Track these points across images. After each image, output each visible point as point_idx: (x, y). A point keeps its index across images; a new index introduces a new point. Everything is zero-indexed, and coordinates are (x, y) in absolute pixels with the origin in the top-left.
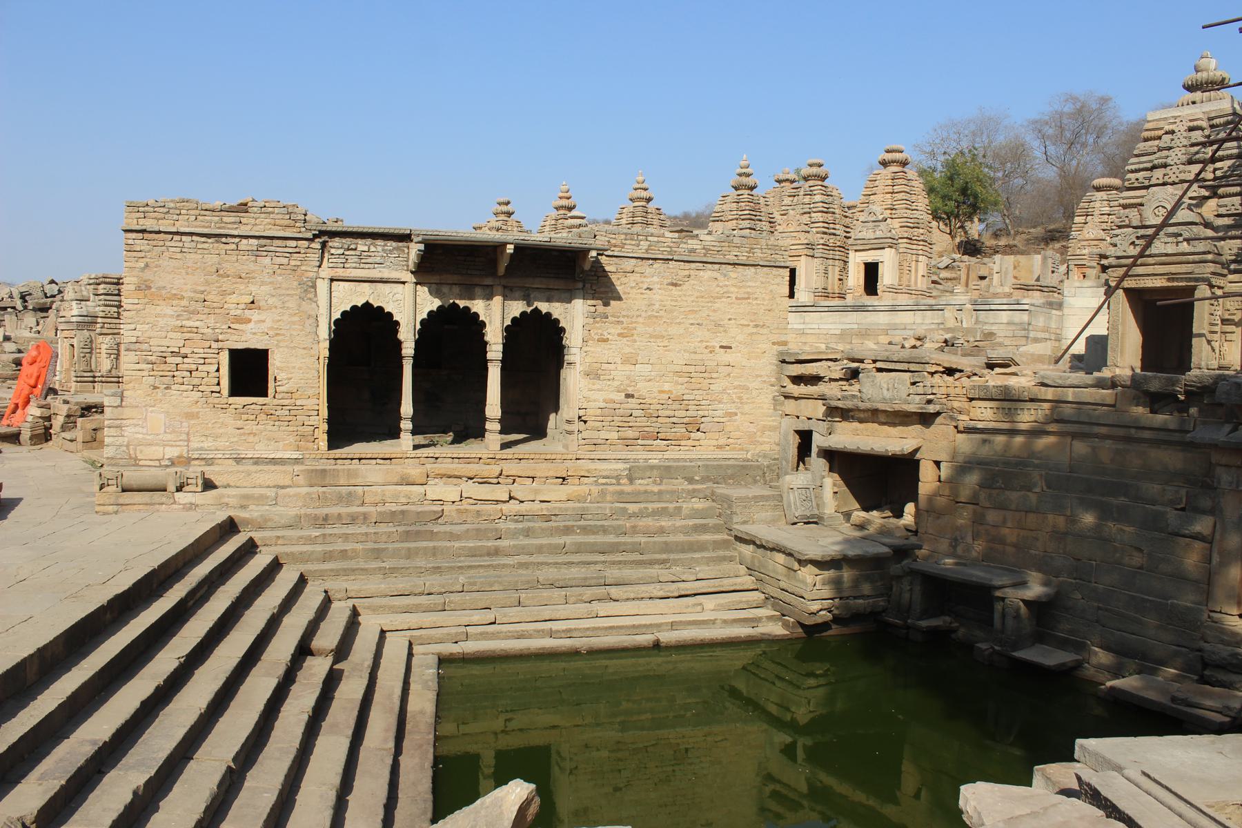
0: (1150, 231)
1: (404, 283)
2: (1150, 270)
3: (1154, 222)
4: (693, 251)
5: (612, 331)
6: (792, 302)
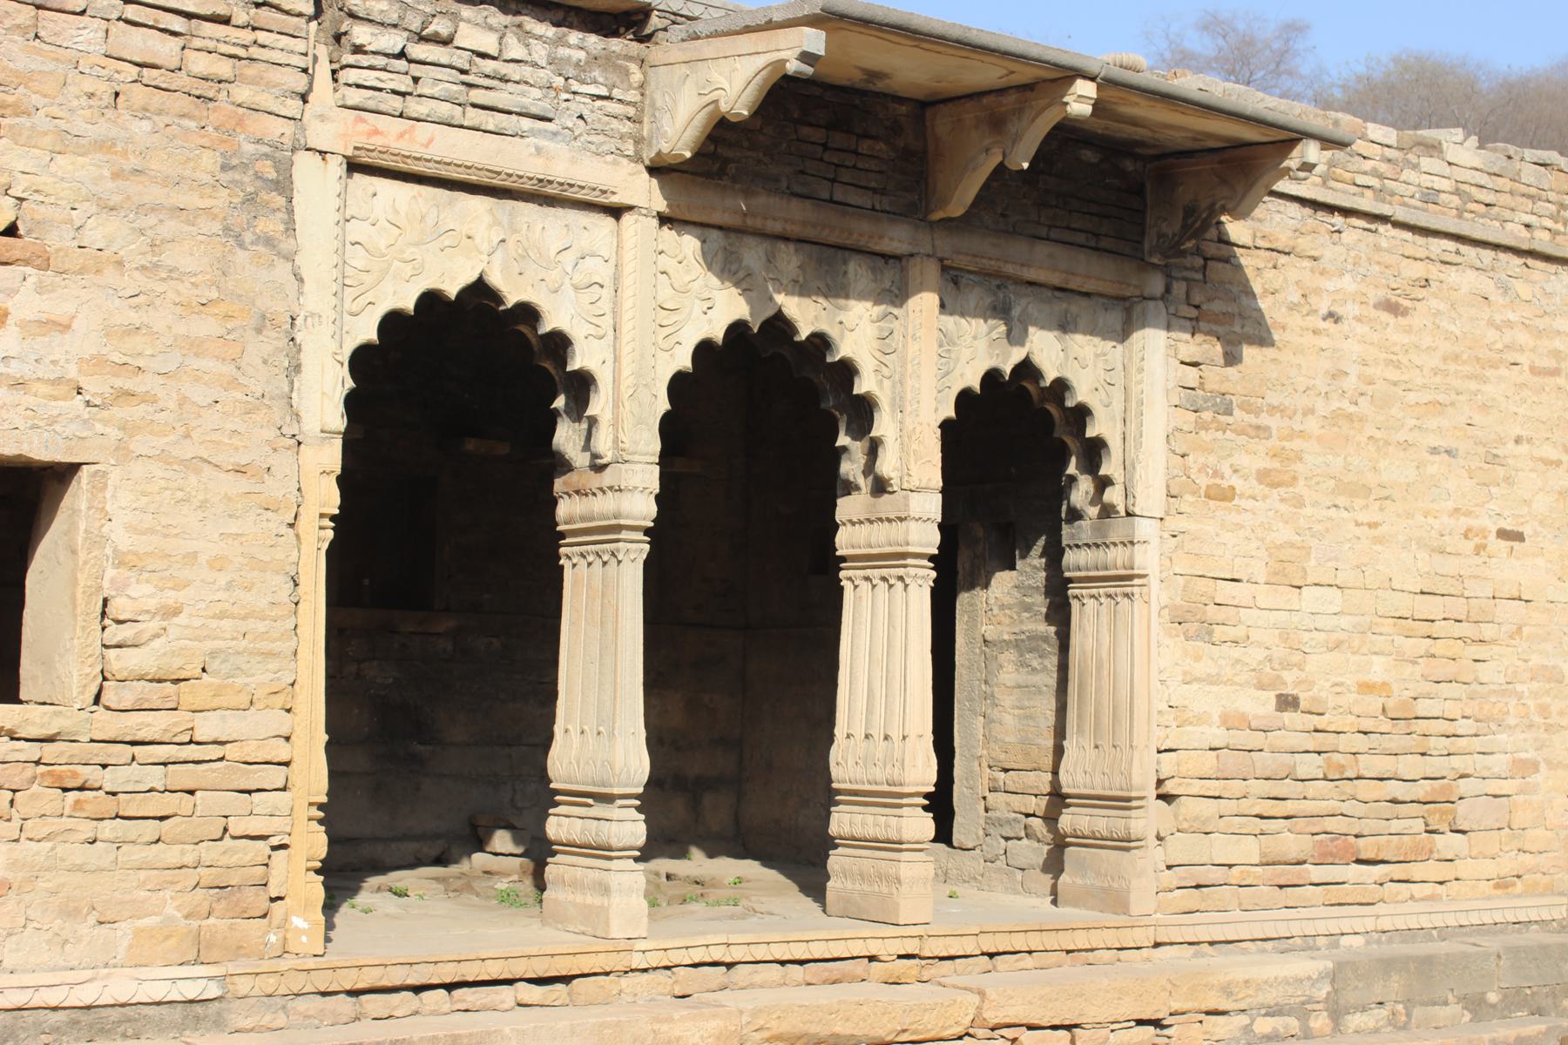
1: (616, 212)
4: (1430, 197)
5: (1243, 460)
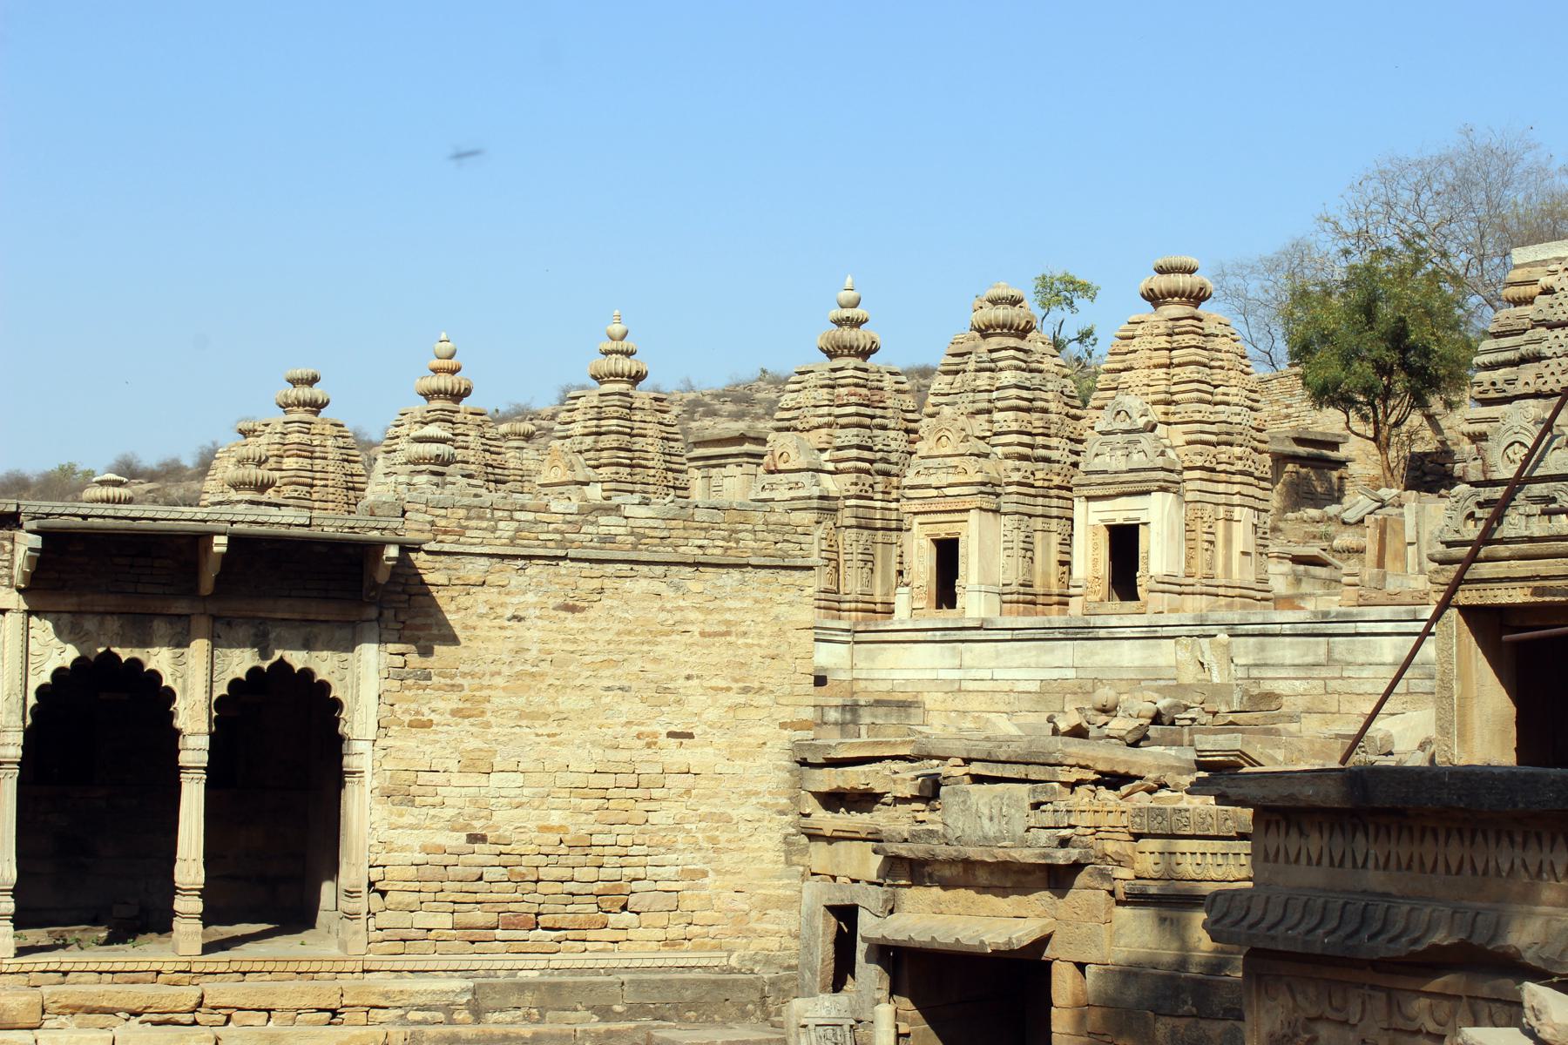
0: (1499, 493)
2: (1501, 569)
4: (608, 539)
5: (441, 705)
6: (946, 617)
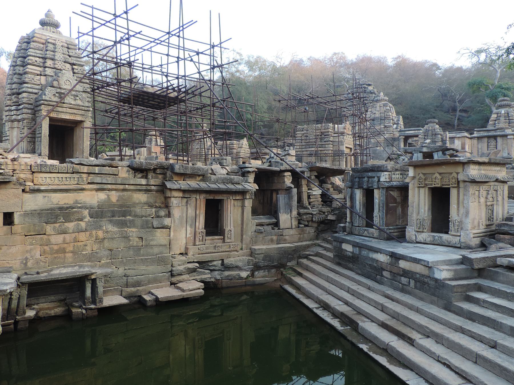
0: (63, 91)
2: (64, 110)
3: (65, 87)
